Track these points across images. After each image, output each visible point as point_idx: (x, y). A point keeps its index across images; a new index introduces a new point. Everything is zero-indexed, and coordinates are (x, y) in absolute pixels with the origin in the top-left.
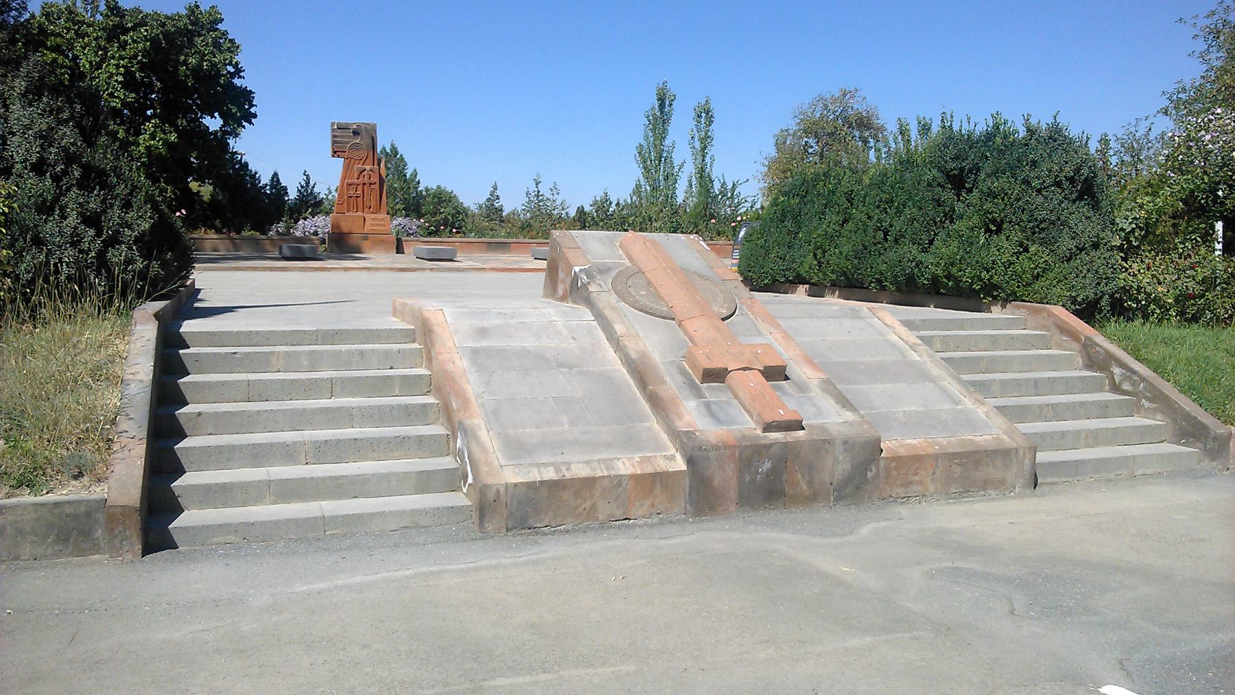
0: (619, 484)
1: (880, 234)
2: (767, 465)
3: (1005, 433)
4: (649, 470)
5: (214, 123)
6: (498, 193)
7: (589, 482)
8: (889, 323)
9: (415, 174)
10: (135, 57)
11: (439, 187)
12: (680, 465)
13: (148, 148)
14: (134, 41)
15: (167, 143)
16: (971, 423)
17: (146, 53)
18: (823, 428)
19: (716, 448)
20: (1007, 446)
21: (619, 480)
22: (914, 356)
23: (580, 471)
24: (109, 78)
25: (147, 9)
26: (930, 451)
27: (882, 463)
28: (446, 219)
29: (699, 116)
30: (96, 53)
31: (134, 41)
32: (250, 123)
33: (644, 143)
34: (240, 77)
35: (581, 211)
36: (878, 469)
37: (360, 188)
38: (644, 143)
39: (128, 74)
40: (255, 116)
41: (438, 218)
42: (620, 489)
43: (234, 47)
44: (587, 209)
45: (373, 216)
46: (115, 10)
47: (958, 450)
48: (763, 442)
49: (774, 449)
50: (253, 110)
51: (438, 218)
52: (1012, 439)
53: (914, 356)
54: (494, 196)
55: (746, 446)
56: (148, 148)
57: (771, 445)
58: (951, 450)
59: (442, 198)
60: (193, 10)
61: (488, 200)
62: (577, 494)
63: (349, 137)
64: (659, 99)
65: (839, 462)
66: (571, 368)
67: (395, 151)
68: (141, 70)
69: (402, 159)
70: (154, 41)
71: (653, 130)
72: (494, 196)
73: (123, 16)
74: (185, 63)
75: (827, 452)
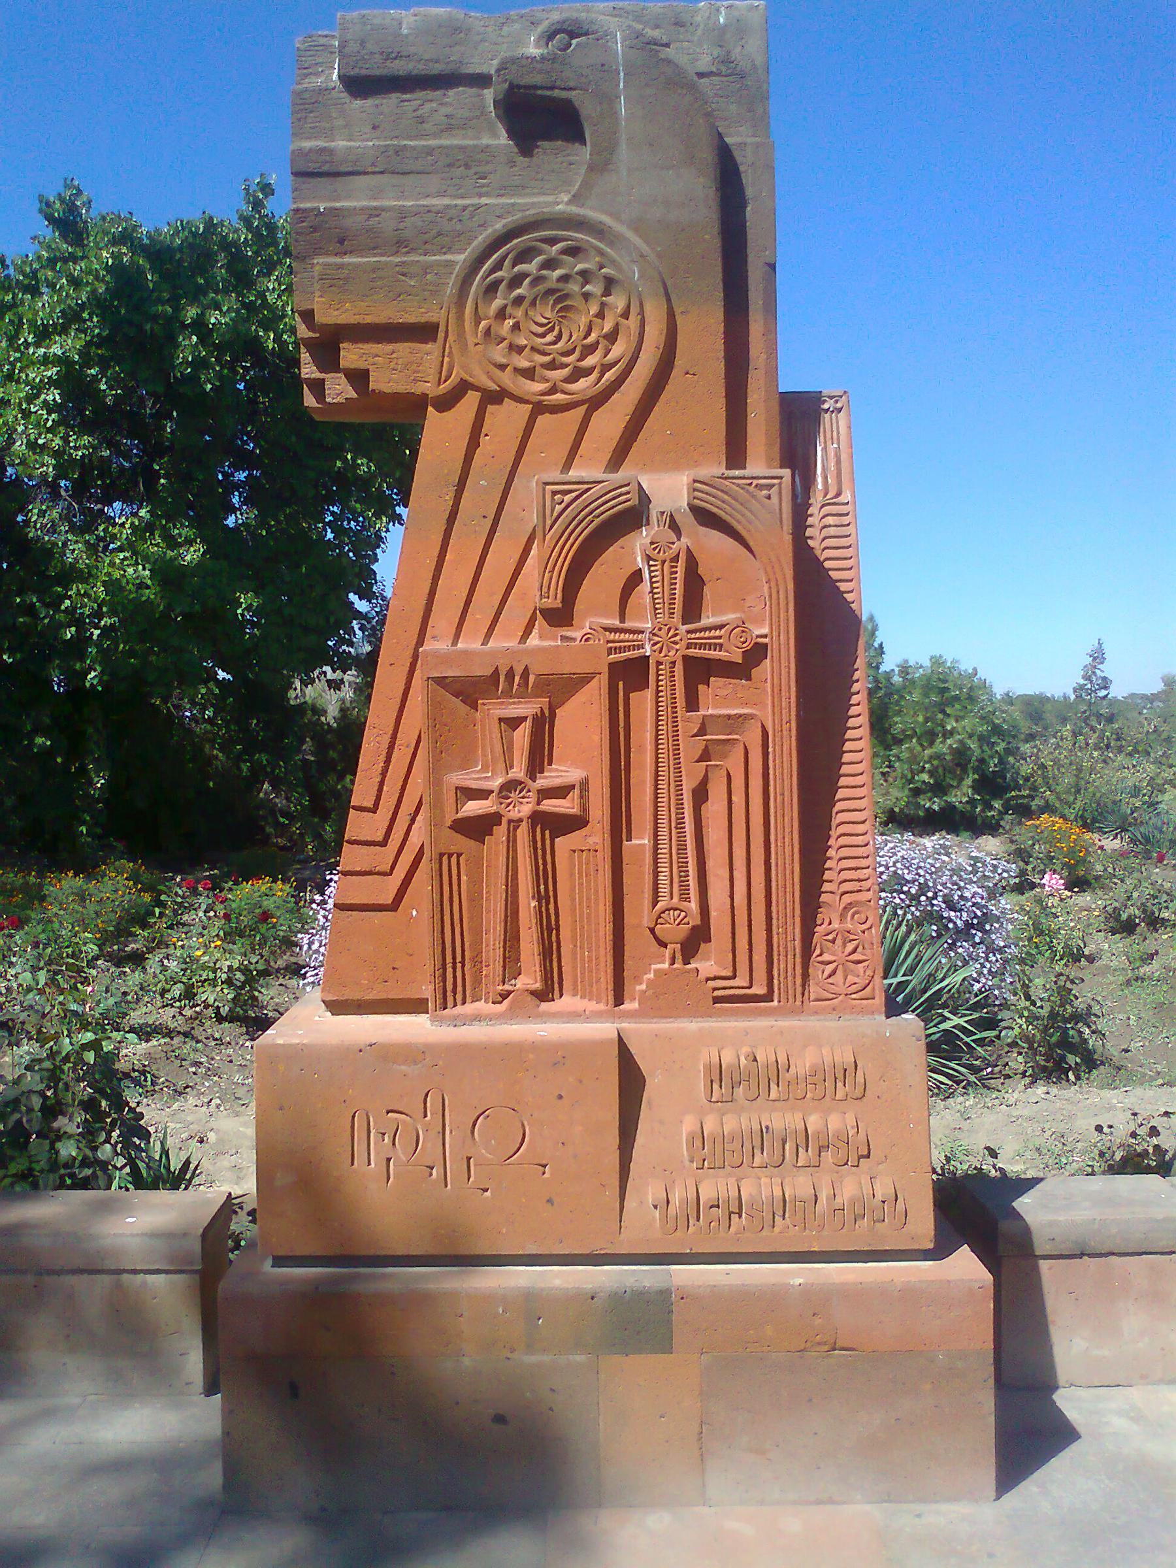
15: (169, 576)
24: (30, 399)
28: (961, 754)
37: (582, 723)
39: (72, 381)
41: (941, 747)
51: (941, 747)
56: (113, 586)
63: (468, 162)
70: (124, 280)
74: (199, 325)
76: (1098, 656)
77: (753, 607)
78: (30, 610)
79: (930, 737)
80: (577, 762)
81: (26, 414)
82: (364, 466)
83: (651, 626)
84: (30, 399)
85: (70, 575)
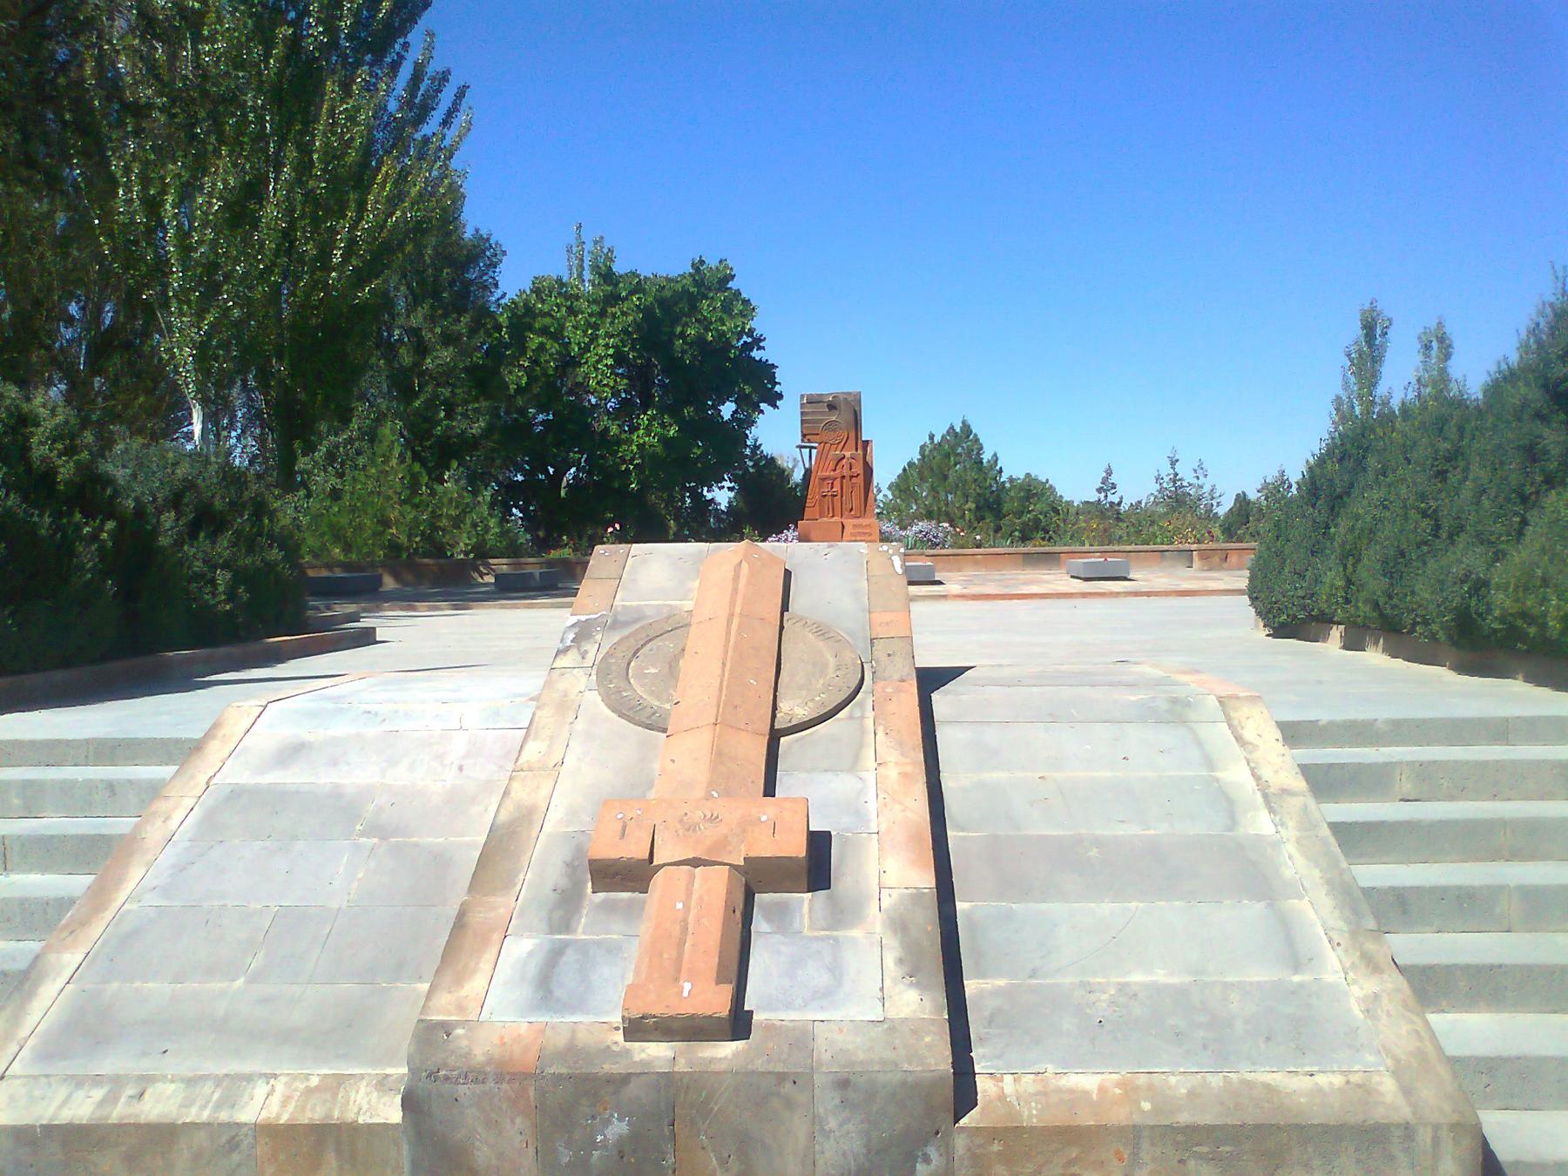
0: (233, 1145)
1: (1426, 524)
2: (618, 1128)
3: (1396, 1073)
4: (314, 1113)
5: (727, 409)
6: (1113, 479)
7: (163, 1135)
8: (1249, 734)
9: (996, 458)
10: (625, 331)
11: (1028, 475)
12: (391, 1112)
13: (641, 447)
14: (624, 314)
15: (664, 440)
16: (1298, 1024)
17: (638, 326)
18: (801, 1038)
19: (475, 1076)
20: (1379, 1115)
21: (229, 1138)
22: (1261, 823)
23: (160, 1104)
24: (598, 362)
25: (645, 272)
26: (1119, 1116)
27: (960, 1144)
28: (1037, 521)
29: (1428, 347)
30: (585, 332)
31: (624, 314)
32: (775, 406)
33: (1341, 393)
34: (760, 348)
35: (1242, 499)
36: (949, 1156)
38: (1341, 393)
40: (780, 396)
42: (236, 1157)
43: (748, 309)
44: (1253, 496)
45: (856, 521)
46: (607, 276)
47: (1208, 1119)
48: (609, 1068)
49: (632, 1089)
50: (777, 389)
52: (1407, 1091)
53: (1261, 823)
54: (1107, 486)
55: (558, 1078)
56: (641, 447)
57: (626, 1079)
58: (1184, 1118)
59: (1032, 490)
60: (698, 265)
61: (1099, 490)
62: (131, 1159)
63: (822, 413)
64: (1364, 327)
65: (827, 1134)
66: (384, 838)
67: (966, 428)
68: (633, 349)
69: (977, 440)
70: (647, 312)
71: (1358, 374)
72: (1107, 486)
73: (616, 285)
74: (682, 335)
75: (789, 1104)
76: (1109, 472)
77: (858, 469)
78: (603, 457)
79: (1020, 514)
80: (837, 488)
81: (596, 369)
82: (748, 389)
83: (846, 472)
84: (598, 362)
85: (619, 442)
